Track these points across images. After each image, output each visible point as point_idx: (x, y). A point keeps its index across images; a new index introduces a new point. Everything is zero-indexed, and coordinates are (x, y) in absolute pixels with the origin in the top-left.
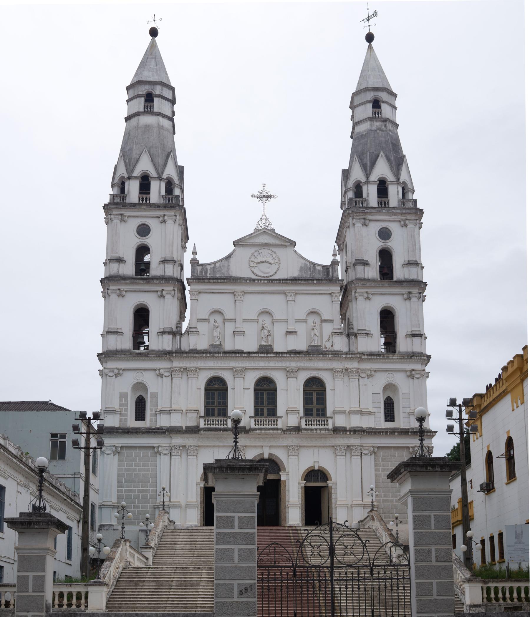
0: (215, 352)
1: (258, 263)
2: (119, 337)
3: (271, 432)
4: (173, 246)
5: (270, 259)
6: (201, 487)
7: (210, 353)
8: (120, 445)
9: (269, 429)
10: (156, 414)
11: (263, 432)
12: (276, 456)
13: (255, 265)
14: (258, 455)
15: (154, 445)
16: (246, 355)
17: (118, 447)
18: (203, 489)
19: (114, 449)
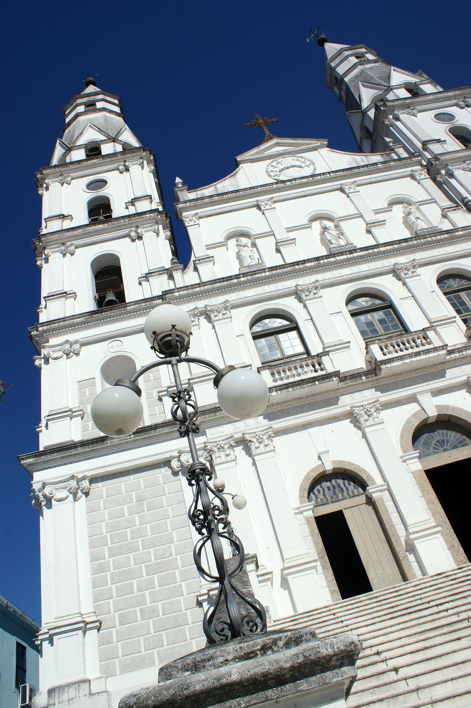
0: (252, 276)
1: (280, 171)
2: (70, 301)
3: (423, 357)
4: (144, 186)
5: (298, 163)
6: (308, 519)
7: (245, 275)
8: (89, 474)
9: (418, 354)
10: (160, 399)
11: (408, 361)
12: (453, 408)
13: (277, 173)
14: (415, 415)
15: (167, 455)
16: (312, 264)
17: (84, 478)
18: (313, 521)
19: (73, 483)
